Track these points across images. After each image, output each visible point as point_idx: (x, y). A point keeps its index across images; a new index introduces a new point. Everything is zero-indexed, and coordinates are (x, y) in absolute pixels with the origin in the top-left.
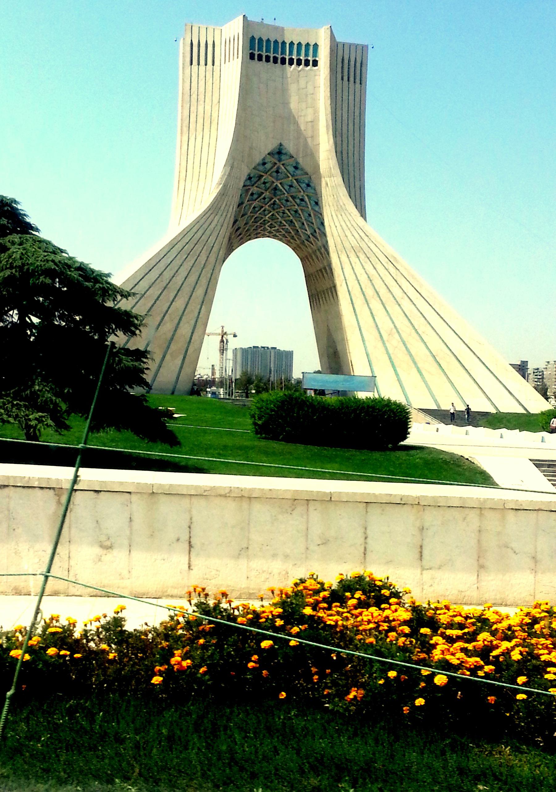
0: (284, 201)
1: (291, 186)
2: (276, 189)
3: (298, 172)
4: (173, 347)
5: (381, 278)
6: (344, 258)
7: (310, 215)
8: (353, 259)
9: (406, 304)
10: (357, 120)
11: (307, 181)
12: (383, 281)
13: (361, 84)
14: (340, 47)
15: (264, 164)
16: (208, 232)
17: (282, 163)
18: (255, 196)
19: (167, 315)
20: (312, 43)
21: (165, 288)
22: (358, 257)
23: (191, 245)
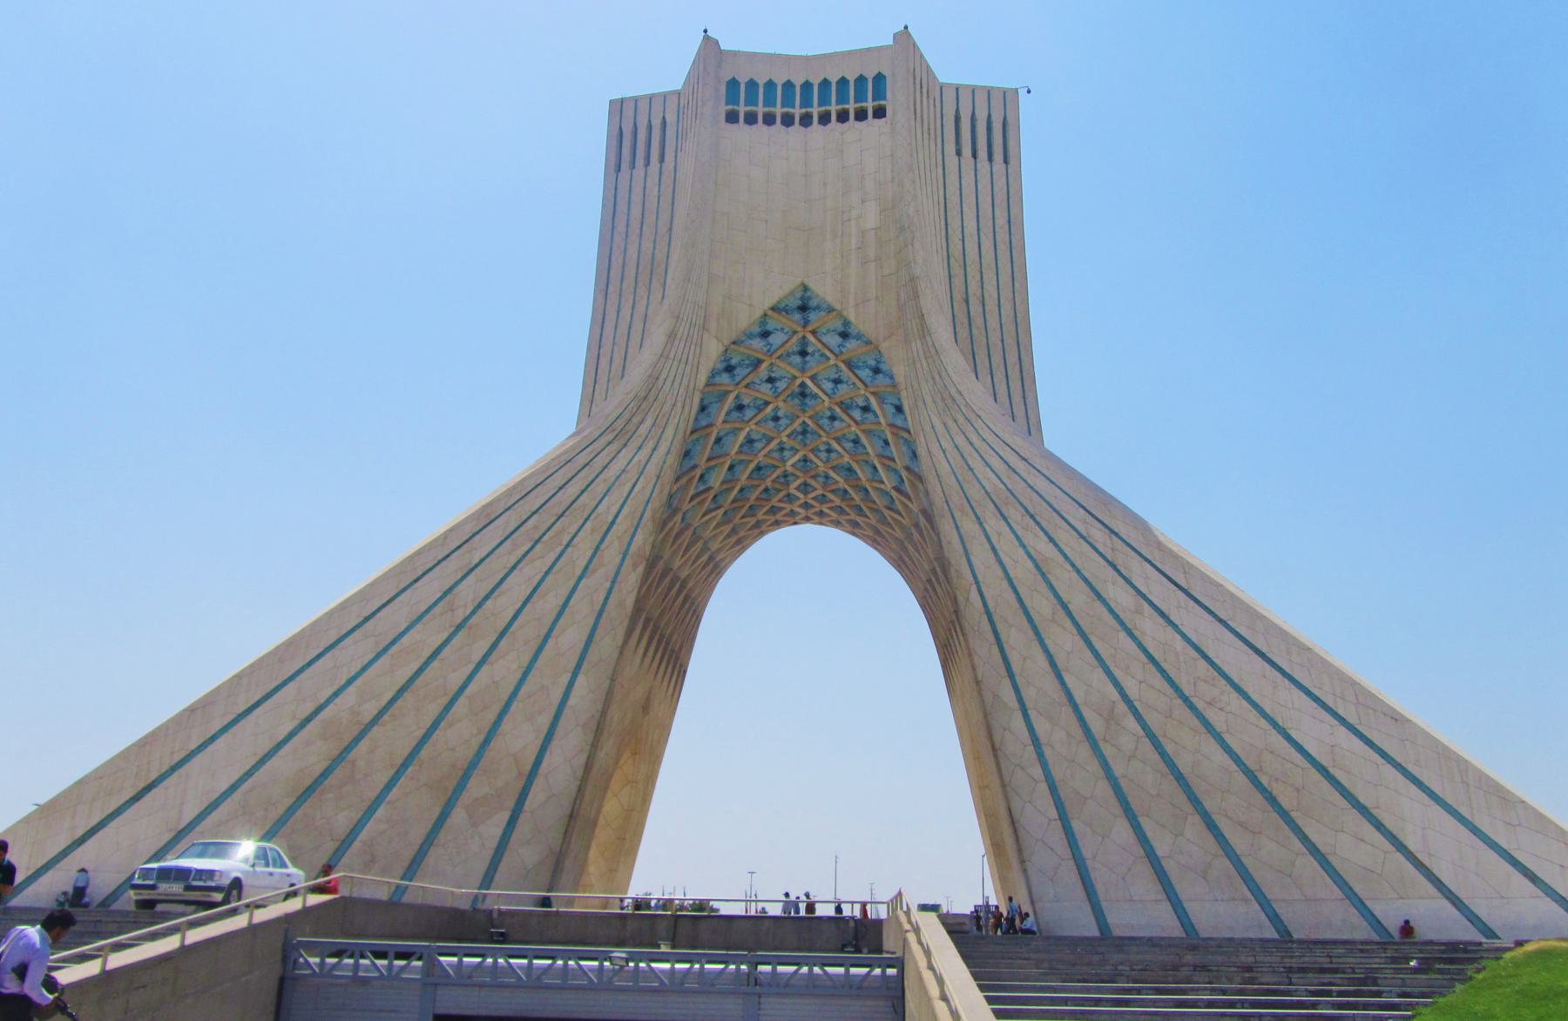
0: (825, 422)
1: (837, 381)
2: (803, 394)
3: (852, 344)
4: (477, 787)
5: (1073, 565)
6: (969, 526)
7: (886, 443)
8: (993, 523)
9: (1150, 628)
10: (1002, 236)
11: (873, 363)
12: (1078, 571)
13: (1006, 162)
14: (949, 97)
15: (765, 334)
16: (599, 487)
17: (810, 328)
18: (749, 413)
19: (462, 700)
20: (870, 75)
21: (459, 627)
22: (1005, 519)
23: (545, 519)
